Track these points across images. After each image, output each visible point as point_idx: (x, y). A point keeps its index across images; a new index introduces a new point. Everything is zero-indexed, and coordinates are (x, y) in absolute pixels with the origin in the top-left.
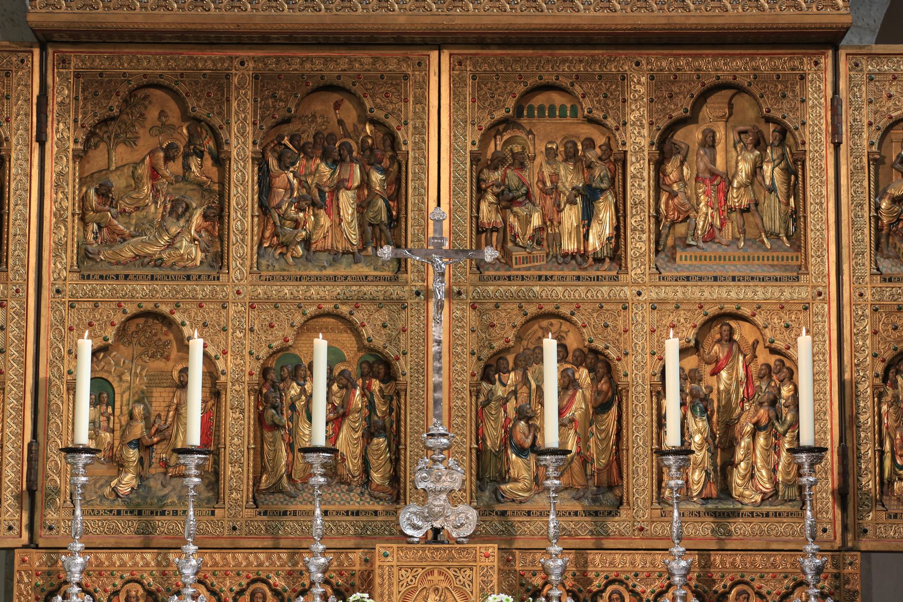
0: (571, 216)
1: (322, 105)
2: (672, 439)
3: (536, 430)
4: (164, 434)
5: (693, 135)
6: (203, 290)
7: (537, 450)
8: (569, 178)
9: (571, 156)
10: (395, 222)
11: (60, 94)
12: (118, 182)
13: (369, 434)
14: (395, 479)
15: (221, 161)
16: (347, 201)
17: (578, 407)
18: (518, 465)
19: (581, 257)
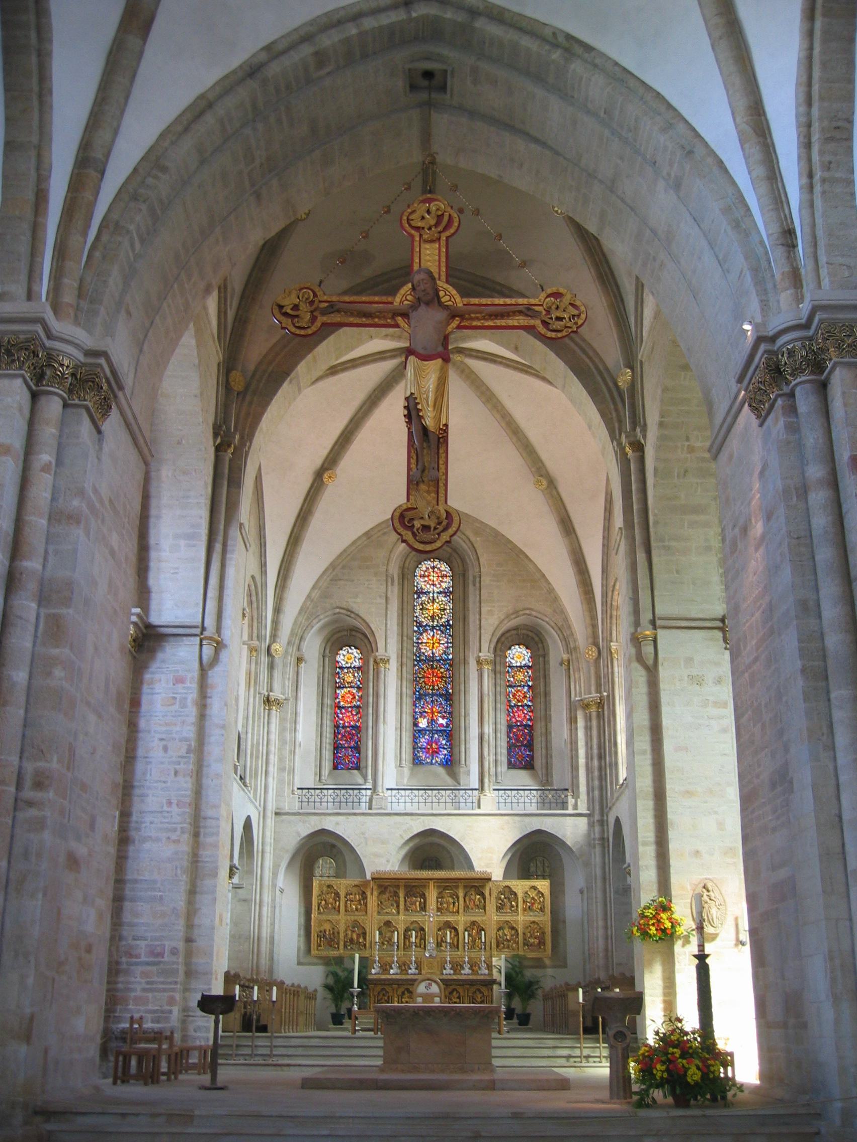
0: (452, 906)
1: (414, 889)
2: (466, 941)
3: (446, 939)
4: (390, 940)
5: (469, 894)
6: (396, 917)
7: (446, 942)
8: (451, 900)
9: (451, 897)
10: (425, 906)
11: (375, 887)
12: (383, 901)
13: (421, 940)
14: (425, 947)
15: (399, 898)
16: (418, 903)
17: (452, 936)
18: (444, 944)
19: (453, 912)
